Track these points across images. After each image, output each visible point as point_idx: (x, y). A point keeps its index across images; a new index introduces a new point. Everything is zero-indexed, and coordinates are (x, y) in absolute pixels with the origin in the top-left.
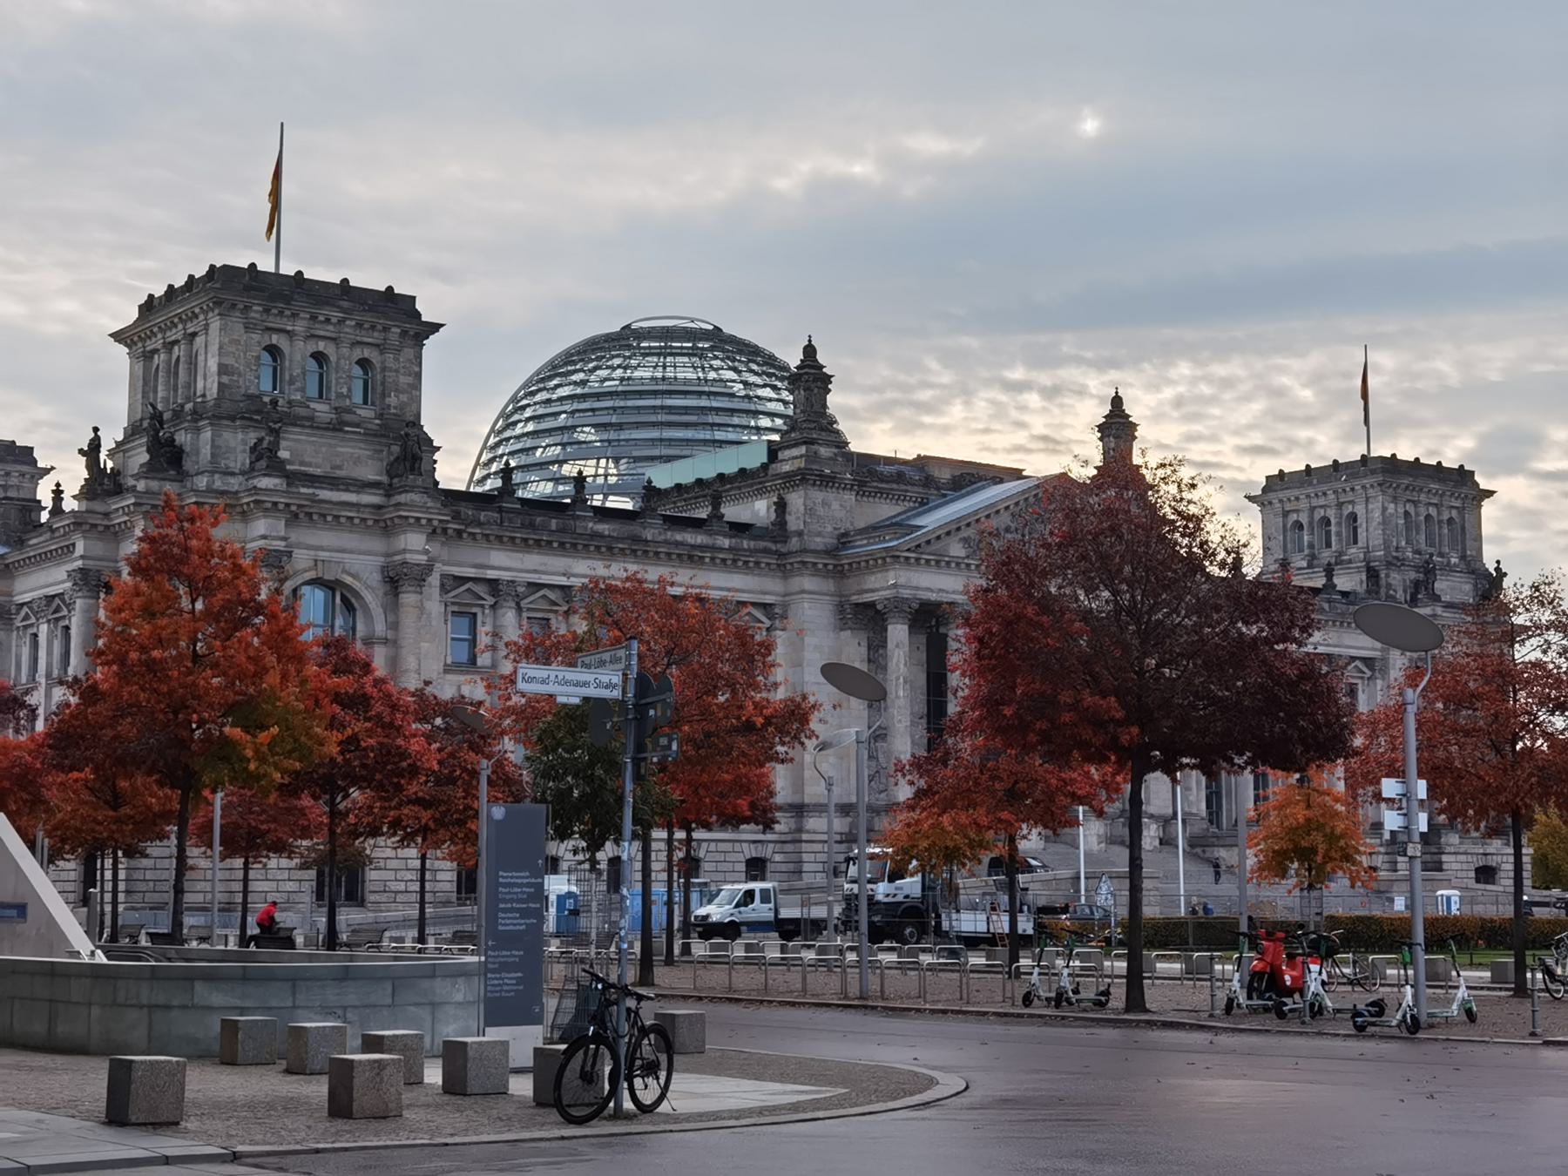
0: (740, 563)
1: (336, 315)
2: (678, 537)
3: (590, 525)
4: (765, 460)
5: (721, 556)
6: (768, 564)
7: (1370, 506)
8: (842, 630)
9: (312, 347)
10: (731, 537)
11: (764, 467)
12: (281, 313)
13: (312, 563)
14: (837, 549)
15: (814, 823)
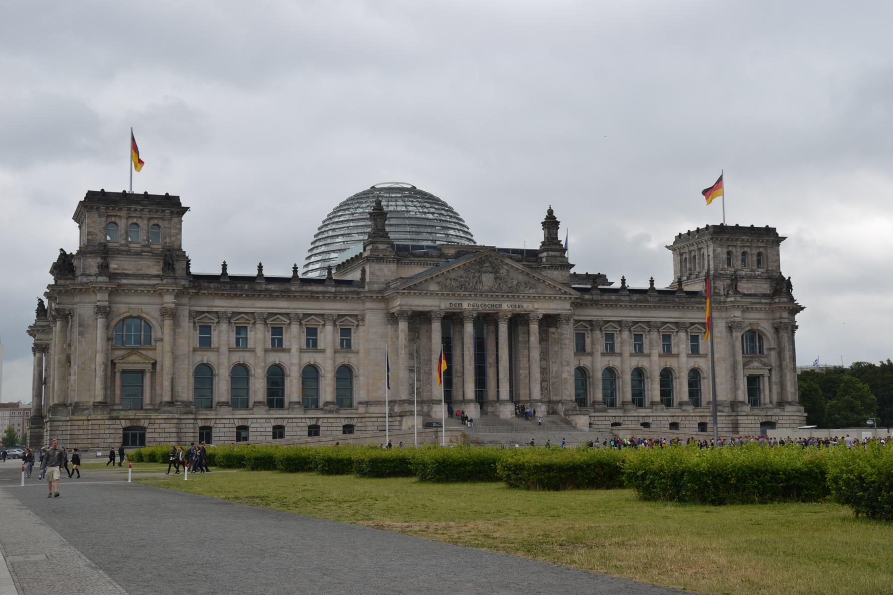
0: (338, 298)
1: (139, 207)
2: (309, 288)
3: (264, 286)
4: (362, 251)
5: (328, 295)
6: (352, 298)
7: (709, 250)
8: (388, 324)
9: (130, 221)
10: (335, 287)
11: (361, 254)
12: (114, 209)
13: (127, 310)
14: (386, 289)
15: (373, 409)
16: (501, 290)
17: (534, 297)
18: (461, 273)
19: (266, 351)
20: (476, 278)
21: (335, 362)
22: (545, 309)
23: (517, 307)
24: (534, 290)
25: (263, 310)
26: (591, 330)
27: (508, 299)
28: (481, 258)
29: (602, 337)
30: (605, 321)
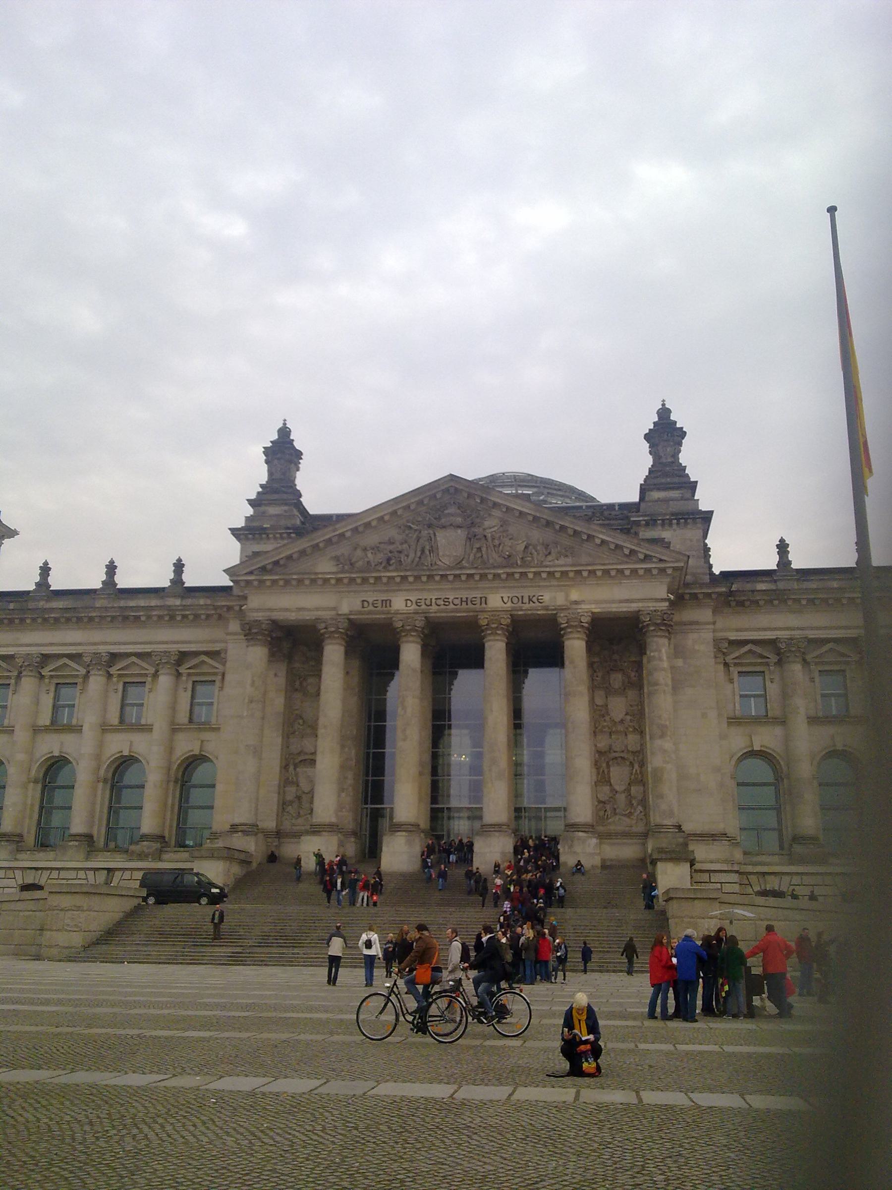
0: (179, 618)
2: (132, 603)
5: (155, 613)
10: (183, 598)
16: (484, 563)
17: (564, 574)
18: (393, 533)
19: (36, 730)
20: (421, 541)
21: (171, 750)
22: (596, 602)
23: (526, 600)
24: (569, 560)
25: (34, 650)
26: (779, 663)
27: (496, 584)
28: (435, 496)
29: (812, 680)
30: (810, 641)
